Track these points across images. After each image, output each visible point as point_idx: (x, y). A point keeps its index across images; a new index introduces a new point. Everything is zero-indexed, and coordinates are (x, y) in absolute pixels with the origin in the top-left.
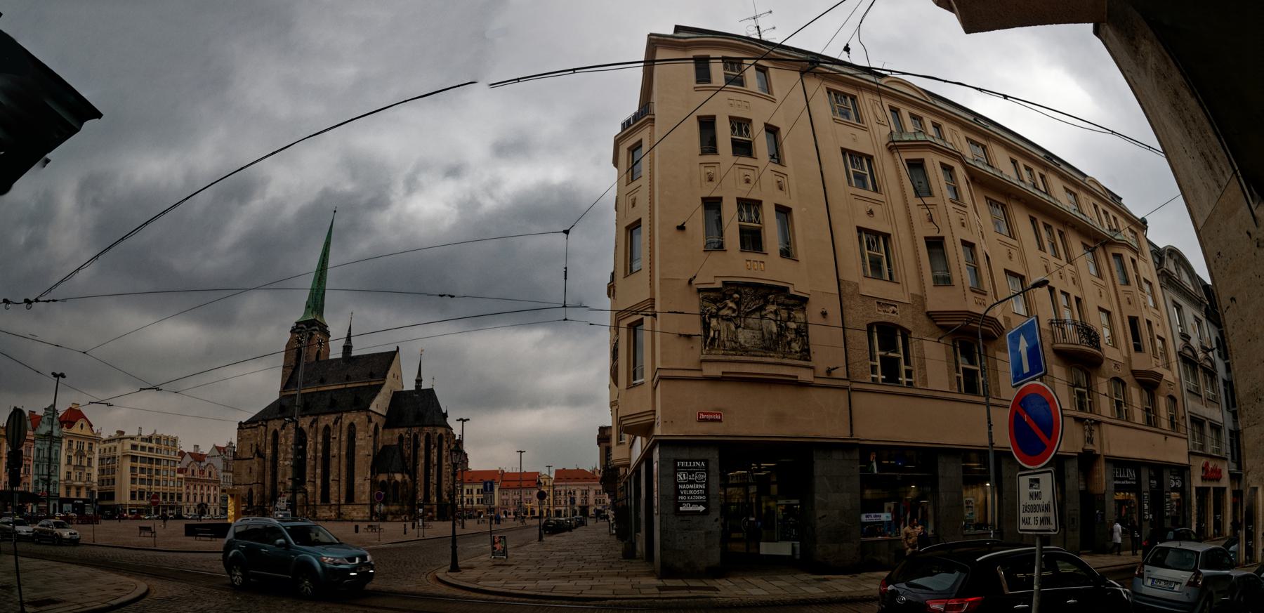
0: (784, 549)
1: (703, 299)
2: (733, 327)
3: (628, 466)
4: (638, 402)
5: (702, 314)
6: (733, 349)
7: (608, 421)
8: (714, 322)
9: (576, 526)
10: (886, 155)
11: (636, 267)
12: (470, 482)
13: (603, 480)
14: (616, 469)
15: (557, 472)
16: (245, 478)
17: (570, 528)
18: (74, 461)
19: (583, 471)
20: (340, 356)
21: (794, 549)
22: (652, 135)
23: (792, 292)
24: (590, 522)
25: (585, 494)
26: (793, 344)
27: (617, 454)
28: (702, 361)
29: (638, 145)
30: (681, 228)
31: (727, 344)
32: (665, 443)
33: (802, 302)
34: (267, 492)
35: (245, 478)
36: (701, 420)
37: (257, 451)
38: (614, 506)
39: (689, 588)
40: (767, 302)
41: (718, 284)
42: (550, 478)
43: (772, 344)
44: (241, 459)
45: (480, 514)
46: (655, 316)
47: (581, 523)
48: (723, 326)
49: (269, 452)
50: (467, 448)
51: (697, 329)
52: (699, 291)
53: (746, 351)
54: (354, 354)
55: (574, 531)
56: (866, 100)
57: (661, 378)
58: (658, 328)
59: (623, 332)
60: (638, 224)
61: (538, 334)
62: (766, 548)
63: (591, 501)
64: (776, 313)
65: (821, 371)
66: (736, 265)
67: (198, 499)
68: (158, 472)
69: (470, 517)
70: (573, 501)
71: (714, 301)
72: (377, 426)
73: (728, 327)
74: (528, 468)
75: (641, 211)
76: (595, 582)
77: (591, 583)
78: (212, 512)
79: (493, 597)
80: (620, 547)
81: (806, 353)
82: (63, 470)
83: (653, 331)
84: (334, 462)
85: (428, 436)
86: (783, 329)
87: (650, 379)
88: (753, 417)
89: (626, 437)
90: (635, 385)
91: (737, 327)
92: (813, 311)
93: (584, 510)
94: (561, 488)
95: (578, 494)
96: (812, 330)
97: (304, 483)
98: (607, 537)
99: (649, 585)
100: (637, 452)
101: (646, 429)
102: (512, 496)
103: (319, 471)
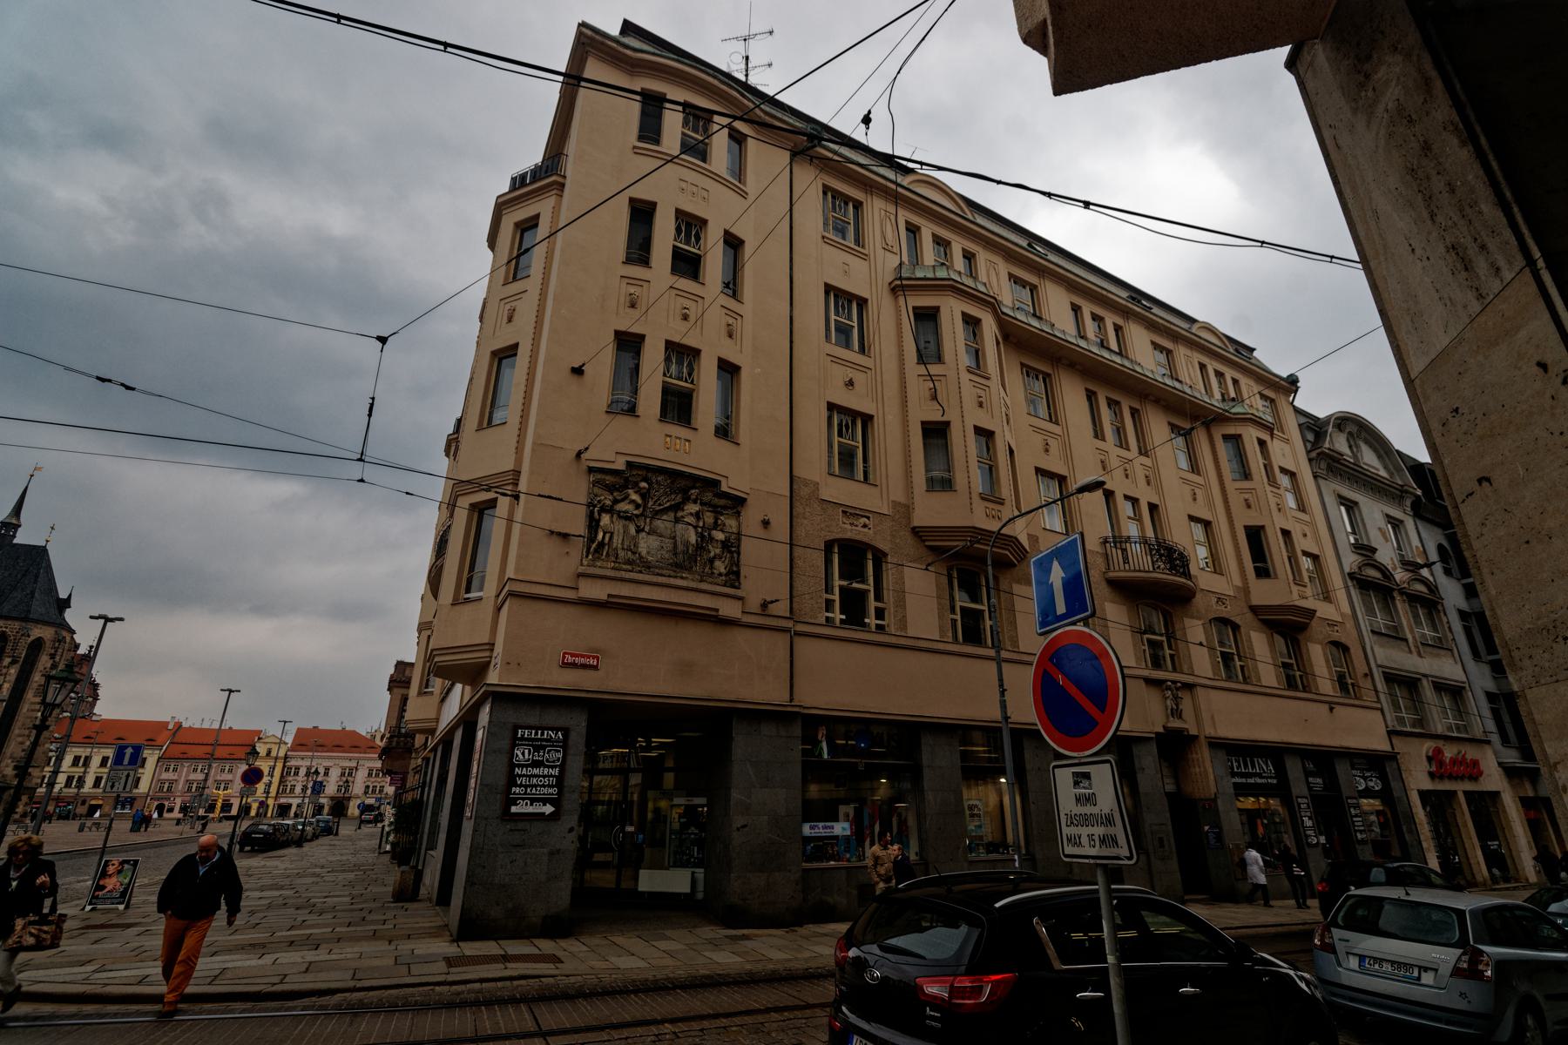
0: (677, 881)
1: (595, 483)
2: (632, 530)
3: (432, 731)
4: (466, 628)
5: (590, 505)
6: (629, 562)
7: (410, 654)
8: (605, 519)
9: (315, 837)
10: (887, 300)
11: (498, 416)
12: (88, 741)
13: (386, 753)
14: (411, 735)
15: (299, 731)
17: (300, 842)
19: (354, 733)
21: (694, 882)
22: (556, 210)
23: (724, 488)
24: (346, 829)
25: (348, 774)
26: (717, 563)
27: (417, 710)
28: (580, 575)
29: (531, 224)
30: (578, 371)
31: (621, 554)
32: (501, 698)
33: (737, 503)
36: (565, 665)
38: (397, 801)
39: (506, 958)
40: (686, 499)
41: (620, 465)
42: (281, 742)
43: (686, 561)
45: (93, 809)
46: (517, 497)
47: (328, 831)
48: (618, 526)
50: (99, 672)
51: (579, 526)
52: (591, 470)
53: (647, 566)
55: (307, 847)
56: (876, 210)
57: (511, 594)
58: (518, 516)
59: (461, 515)
60: (511, 351)
63: (358, 788)
64: (697, 515)
65: (754, 604)
66: (650, 439)
69: (64, 817)
70: (318, 788)
71: (610, 489)
73: (625, 527)
74: (235, 722)
75: (520, 332)
76: (321, 955)
77: (311, 956)
79: (47, 1008)
80: (393, 875)
81: (734, 577)
83: (510, 520)
86: (705, 539)
87: (494, 593)
88: (646, 666)
89: (438, 684)
90: (468, 601)
91: (639, 530)
92: (751, 518)
93: (339, 807)
94: (302, 762)
95: (335, 774)
96: (747, 546)
98: (371, 857)
99: (430, 952)
100: (452, 709)
101: (473, 673)
102: (186, 774)
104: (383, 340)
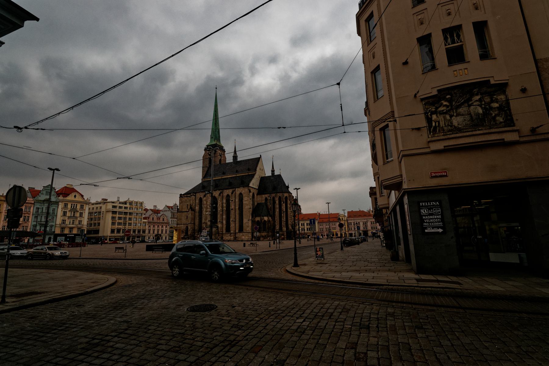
0: (513, 258)
1: (425, 104)
2: (448, 117)
3: (388, 208)
4: (390, 172)
5: (426, 113)
6: (449, 131)
7: (374, 184)
8: (434, 117)
9: (362, 242)
11: (380, 94)
12: (303, 220)
13: (375, 216)
14: (381, 209)
15: (348, 212)
16: (184, 221)
17: (358, 243)
18: (68, 214)
19: (363, 211)
20: (232, 161)
21: (521, 258)
22: (379, 5)
23: (492, 82)
24: (370, 240)
25: (365, 224)
26: (498, 118)
27: (381, 202)
28: (429, 142)
29: (371, 16)
30: (406, 63)
31: (445, 128)
32: (411, 193)
33: (502, 87)
34: (197, 228)
35: (184, 221)
36: (432, 177)
37: (191, 208)
38: (383, 230)
39: (438, 281)
40: (473, 95)
41: (435, 92)
42: (345, 216)
43: (477, 123)
44: (181, 212)
45: (309, 236)
46: (395, 121)
47: (364, 240)
48: (441, 118)
49: (197, 208)
50: (300, 203)
51: (423, 123)
52: (422, 100)
53: (459, 130)
54: (239, 159)
55: (361, 245)
57: (404, 156)
58: (398, 127)
59: (377, 133)
60: (378, 68)
61: (331, 142)
62: (493, 257)
63: (369, 228)
64: (480, 100)
65: (526, 130)
67: (156, 232)
68: (130, 219)
69: (304, 238)
70: (359, 228)
71: (433, 104)
72: (253, 194)
73: (445, 118)
74: (332, 211)
75: (379, 60)
76: (375, 274)
77: (373, 275)
78: (164, 238)
81: (510, 122)
82: (59, 220)
83: (395, 130)
84: (232, 212)
85: (280, 198)
86: (487, 110)
87: (397, 157)
89: (385, 192)
90: (388, 162)
91: (451, 116)
92: (513, 91)
93: (366, 233)
94: (352, 221)
95: (361, 224)
96: (514, 105)
97: (217, 223)
98: (380, 248)
99: (410, 278)
100: (393, 198)
101: (397, 186)
102: (325, 226)
103: (224, 217)
104: (339, 84)
